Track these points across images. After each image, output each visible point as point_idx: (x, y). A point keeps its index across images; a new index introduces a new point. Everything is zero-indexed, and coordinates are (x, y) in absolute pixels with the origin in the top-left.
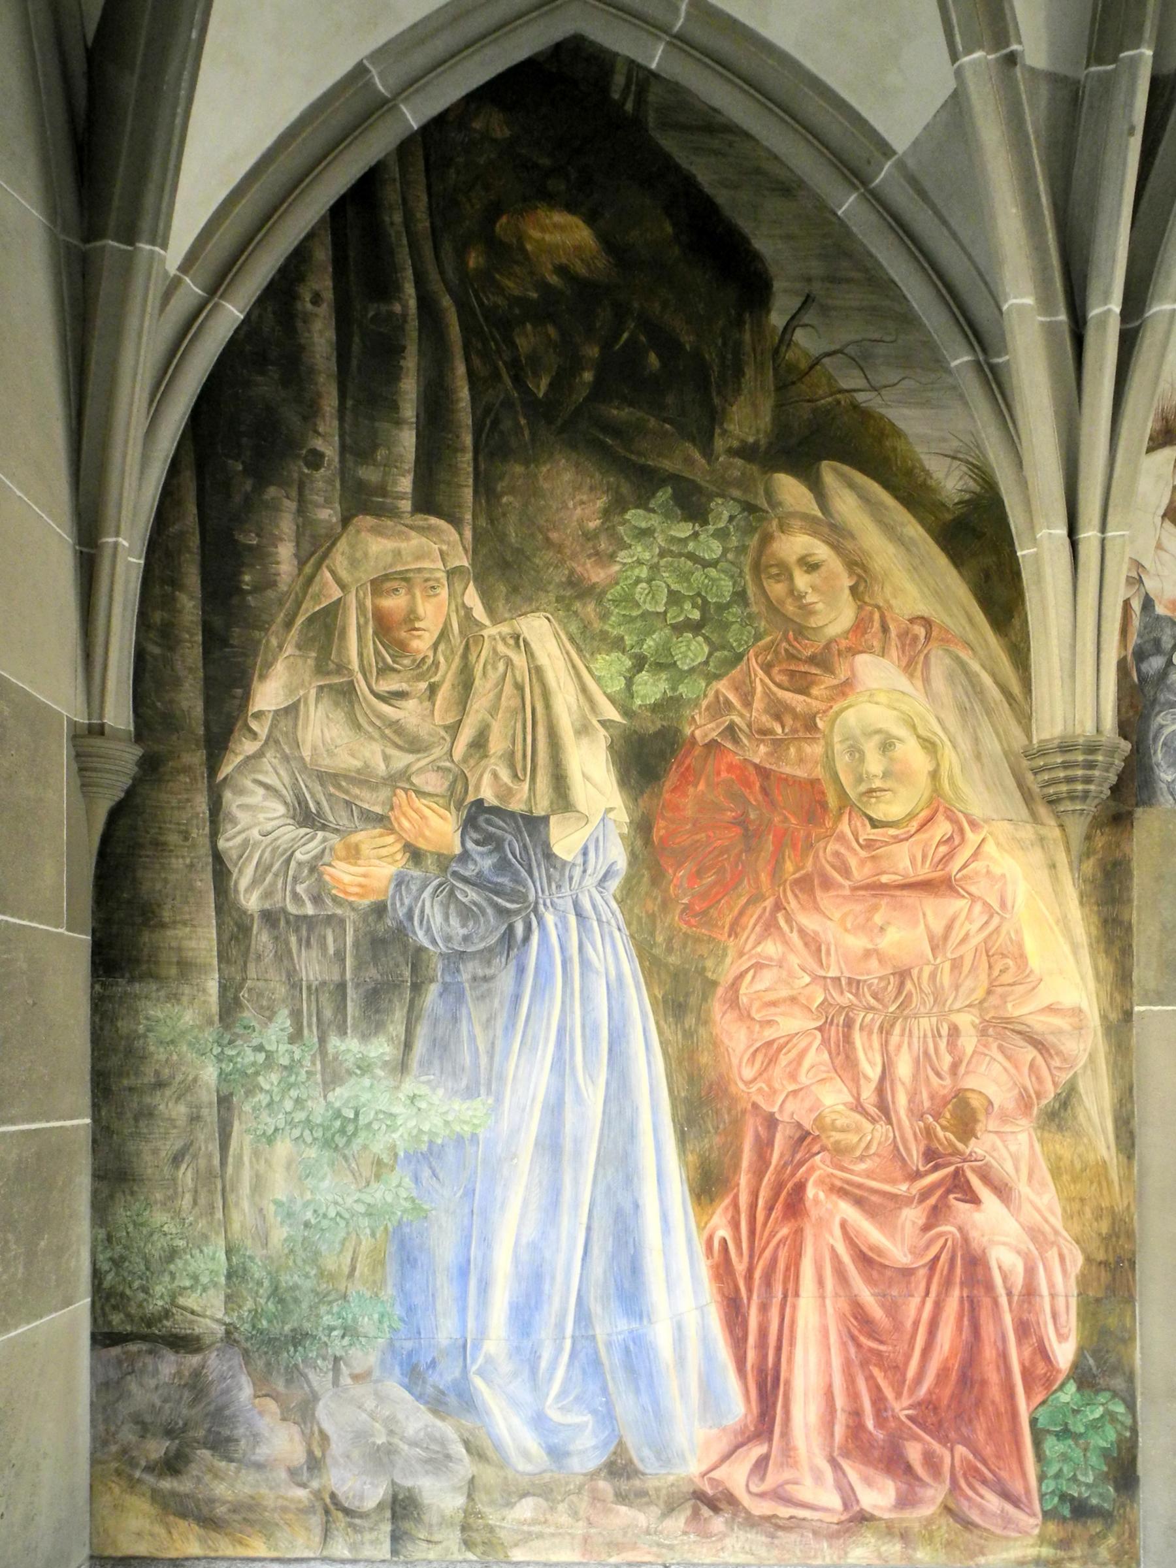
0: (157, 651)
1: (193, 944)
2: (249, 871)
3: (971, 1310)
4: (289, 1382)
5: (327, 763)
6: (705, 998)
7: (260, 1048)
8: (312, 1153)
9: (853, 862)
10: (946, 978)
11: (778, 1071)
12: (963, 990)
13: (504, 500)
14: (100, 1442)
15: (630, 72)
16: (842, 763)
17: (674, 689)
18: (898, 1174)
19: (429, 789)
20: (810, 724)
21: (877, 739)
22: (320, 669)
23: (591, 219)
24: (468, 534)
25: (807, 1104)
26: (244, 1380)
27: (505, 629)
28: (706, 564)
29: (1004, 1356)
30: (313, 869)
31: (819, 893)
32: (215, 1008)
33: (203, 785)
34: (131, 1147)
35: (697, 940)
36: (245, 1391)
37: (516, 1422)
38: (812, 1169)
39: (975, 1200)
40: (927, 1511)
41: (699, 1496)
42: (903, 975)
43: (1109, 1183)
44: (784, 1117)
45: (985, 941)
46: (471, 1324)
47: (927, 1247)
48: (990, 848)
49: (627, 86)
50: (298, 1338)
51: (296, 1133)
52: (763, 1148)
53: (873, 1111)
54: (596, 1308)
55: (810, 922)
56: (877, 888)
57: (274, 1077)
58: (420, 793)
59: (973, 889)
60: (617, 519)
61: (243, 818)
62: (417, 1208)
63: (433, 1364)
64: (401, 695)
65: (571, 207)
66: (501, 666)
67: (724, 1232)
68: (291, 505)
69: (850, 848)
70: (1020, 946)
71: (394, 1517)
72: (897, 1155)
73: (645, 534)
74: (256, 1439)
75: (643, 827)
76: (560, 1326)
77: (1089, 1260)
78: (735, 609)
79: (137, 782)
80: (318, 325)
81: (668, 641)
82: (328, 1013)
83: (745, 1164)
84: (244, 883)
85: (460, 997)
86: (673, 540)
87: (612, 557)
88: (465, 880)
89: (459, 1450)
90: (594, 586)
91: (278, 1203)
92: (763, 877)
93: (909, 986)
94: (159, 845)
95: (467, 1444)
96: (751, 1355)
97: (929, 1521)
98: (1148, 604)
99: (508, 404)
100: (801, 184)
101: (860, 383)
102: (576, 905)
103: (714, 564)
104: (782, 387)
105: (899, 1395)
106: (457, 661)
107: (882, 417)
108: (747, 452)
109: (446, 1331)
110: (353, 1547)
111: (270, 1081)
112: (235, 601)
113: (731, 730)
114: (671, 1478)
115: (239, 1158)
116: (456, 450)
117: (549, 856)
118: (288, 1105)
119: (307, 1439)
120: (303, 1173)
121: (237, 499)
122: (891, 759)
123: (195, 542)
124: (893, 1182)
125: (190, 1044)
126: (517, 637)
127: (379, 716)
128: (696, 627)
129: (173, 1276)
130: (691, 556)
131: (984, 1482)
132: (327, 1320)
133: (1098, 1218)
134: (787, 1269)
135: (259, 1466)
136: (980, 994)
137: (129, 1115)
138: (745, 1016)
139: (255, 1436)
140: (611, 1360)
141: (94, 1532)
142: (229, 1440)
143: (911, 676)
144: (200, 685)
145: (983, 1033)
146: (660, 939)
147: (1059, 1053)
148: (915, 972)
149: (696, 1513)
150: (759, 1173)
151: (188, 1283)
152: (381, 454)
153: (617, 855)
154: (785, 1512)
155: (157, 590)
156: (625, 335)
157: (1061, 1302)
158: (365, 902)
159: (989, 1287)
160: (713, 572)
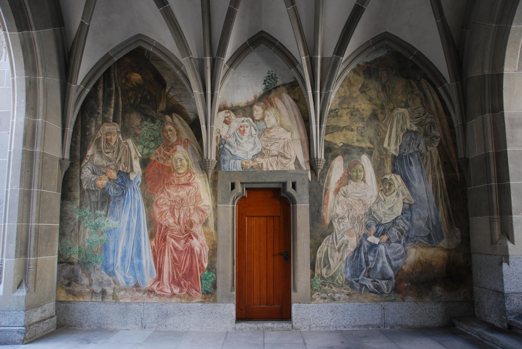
4: (87, 270)
5: (97, 164)
6: (152, 204)
8: (92, 230)
9: (175, 180)
10: (189, 200)
11: (163, 216)
12: (191, 202)
13: (126, 120)
14: (58, 280)
17: (149, 151)
19: (112, 168)
20: (169, 157)
21: (180, 159)
24: (120, 126)
25: (167, 222)
26: (80, 270)
27: (125, 141)
28: (155, 130)
30: (94, 182)
31: (170, 186)
32: (79, 206)
35: (151, 194)
38: (168, 233)
39: (192, 239)
42: (182, 200)
43: (213, 236)
45: (195, 194)
46: (115, 260)
47: (185, 247)
48: (196, 178)
50: (89, 263)
51: (90, 227)
52: (160, 229)
53: (177, 223)
54: (134, 258)
55: (168, 191)
56: (179, 185)
57: (87, 217)
58: (111, 169)
59: (193, 185)
62: (107, 240)
63: (109, 267)
64: (109, 152)
66: (124, 148)
67: (154, 244)
69: (175, 178)
70: (200, 195)
71: (102, 294)
72: (181, 231)
73: (146, 125)
74: (82, 280)
75: (144, 174)
76: (129, 261)
78: (159, 138)
82: (95, 207)
83: (157, 232)
84: (84, 184)
85: (115, 203)
87: (141, 129)
88: (117, 184)
89: (112, 282)
90: (138, 134)
91: (86, 239)
92: (162, 183)
93: (183, 201)
95: (114, 281)
96: (158, 266)
98: (221, 136)
101: (179, 100)
102: (133, 187)
104: (167, 101)
106: (117, 147)
107: (182, 106)
108: (162, 112)
109: (111, 262)
110: (96, 299)
113: (158, 158)
114: (145, 287)
115: (81, 231)
116: (119, 112)
117: (130, 179)
120: (91, 234)
122: (182, 163)
124: (180, 236)
125: (75, 212)
126: (126, 143)
127: (106, 156)
128: (153, 141)
129: (70, 252)
132: (93, 259)
133: (211, 242)
134: (163, 251)
135: (82, 285)
136: (194, 203)
138: (158, 207)
139: (82, 280)
141: (56, 297)
142: (77, 280)
143: (185, 149)
145: (194, 210)
146: (146, 194)
147: (206, 213)
148: (184, 199)
150: (159, 234)
151: (72, 253)
153: (140, 179)
156: (145, 93)
158: (102, 187)
160: (156, 132)
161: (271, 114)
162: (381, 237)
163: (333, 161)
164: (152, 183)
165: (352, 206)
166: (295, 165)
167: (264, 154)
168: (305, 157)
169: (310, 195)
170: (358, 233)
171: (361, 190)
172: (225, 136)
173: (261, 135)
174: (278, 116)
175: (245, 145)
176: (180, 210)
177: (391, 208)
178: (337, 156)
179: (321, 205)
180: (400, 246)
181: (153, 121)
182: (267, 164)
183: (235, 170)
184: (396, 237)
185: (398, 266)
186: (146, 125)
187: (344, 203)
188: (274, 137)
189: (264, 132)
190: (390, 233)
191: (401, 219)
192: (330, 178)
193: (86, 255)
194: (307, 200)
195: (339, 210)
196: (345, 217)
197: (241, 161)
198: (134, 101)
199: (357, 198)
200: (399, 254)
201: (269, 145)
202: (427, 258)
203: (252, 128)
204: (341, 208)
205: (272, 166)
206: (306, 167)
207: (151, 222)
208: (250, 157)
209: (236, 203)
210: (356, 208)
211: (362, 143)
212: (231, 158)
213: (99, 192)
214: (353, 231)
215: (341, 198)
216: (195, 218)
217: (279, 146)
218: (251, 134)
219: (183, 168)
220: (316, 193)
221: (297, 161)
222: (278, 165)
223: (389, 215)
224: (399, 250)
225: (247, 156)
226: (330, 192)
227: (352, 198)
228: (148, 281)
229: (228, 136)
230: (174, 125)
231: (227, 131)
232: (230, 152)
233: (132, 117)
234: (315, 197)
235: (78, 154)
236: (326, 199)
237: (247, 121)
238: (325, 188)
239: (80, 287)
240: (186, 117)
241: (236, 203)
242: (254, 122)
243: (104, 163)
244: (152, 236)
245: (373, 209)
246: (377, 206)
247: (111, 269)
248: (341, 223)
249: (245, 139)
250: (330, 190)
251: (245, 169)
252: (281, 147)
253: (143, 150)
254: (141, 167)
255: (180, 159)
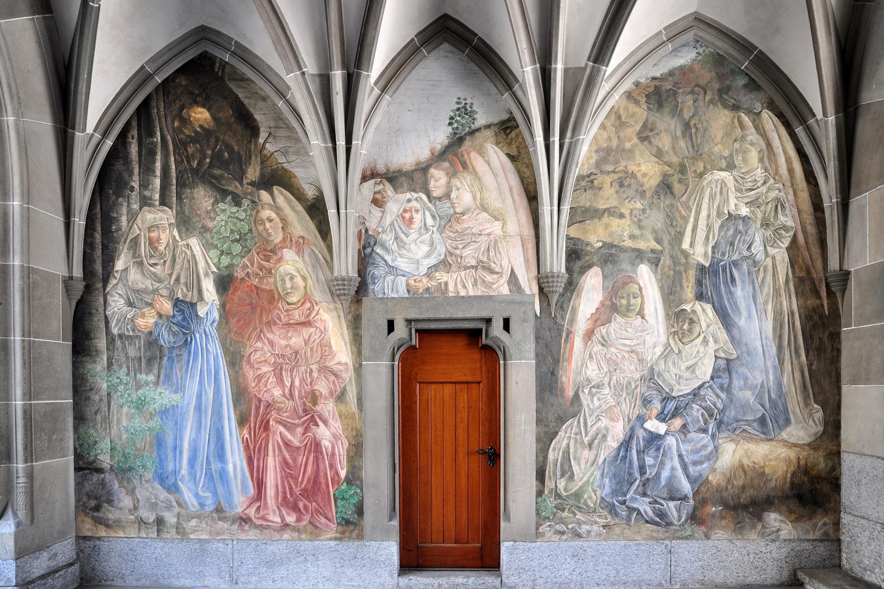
0: (89, 251)
1: (100, 345)
2: (115, 321)
3: (316, 459)
4: (128, 483)
5: (136, 287)
6: (241, 361)
7: (118, 378)
9: (282, 316)
10: (309, 354)
12: (314, 357)
14: (78, 500)
15: (220, 64)
16: (279, 284)
18: (296, 417)
19: (164, 294)
20: (270, 273)
21: (289, 276)
22: (134, 257)
23: (209, 110)
24: (175, 212)
25: (270, 395)
26: (116, 482)
27: (184, 242)
29: (326, 474)
30: (132, 321)
32: (106, 365)
33: (102, 294)
34: (84, 409)
36: (116, 486)
37: (190, 495)
38: (271, 416)
39: (317, 425)
40: (305, 523)
41: (241, 518)
42: (297, 353)
44: (263, 399)
46: (177, 465)
48: (321, 311)
49: (220, 67)
50: (130, 469)
51: (129, 404)
52: (258, 408)
53: (288, 396)
54: (212, 460)
55: (270, 336)
57: (122, 387)
58: (162, 296)
59: (316, 325)
60: (216, 206)
61: (113, 304)
63: (167, 477)
64: (156, 264)
65: (203, 106)
67: (247, 436)
68: (125, 204)
69: (281, 312)
70: (330, 343)
74: (120, 501)
75: (223, 306)
77: (350, 444)
78: (249, 235)
79: (84, 293)
80: (133, 146)
81: (230, 245)
82: (137, 366)
84: (113, 325)
85: (173, 362)
86: (232, 213)
87: (215, 218)
88: (174, 324)
91: (123, 426)
93: (298, 356)
94: (90, 314)
95: (177, 502)
96: (255, 474)
97: (305, 526)
98: (367, 231)
99: (186, 169)
100: (268, 97)
101: (284, 160)
102: (205, 331)
103: (243, 220)
105: (296, 487)
108: (252, 184)
109: (170, 467)
110: (147, 534)
111: (121, 388)
112: (110, 235)
117: (197, 315)
118: (126, 396)
119: (133, 500)
120: (131, 417)
121: (111, 202)
122: (293, 283)
123: (99, 216)
124: (294, 419)
126: (188, 245)
127: (150, 271)
128: (238, 241)
130: (237, 218)
131: (321, 514)
133: (352, 430)
135: (121, 509)
136: (318, 359)
137: (83, 399)
138: (252, 367)
140: (216, 476)
143: (299, 256)
144: (101, 262)
145: (319, 371)
147: (341, 377)
149: (240, 524)
150: (256, 417)
152: (150, 187)
153: (216, 315)
154: (265, 523)
155: (89, 232)
157: (342, 457)
159: (322, 453)
161: (464, 185)
162: (670, 422)
163: (583, 278)
164: (238, 321)
165: (617, 364)
166: (509, 285)
167: (450, 264)
168: (528, 270)
169: (537, 342)
170: (627, 413)
171: (636, 332)
172: (374, 231)
173: (445, 227)
174: (476, 189)
175: (413, 246)
176: (293, 372)
177: (691, 367)
178: (590, 266)
179: (559, 361)
180: (706, 439)
181: (237, 202)
182: (456, 284)
183: (394, 296)
184: (699, 421)
185: (701, 475)
186: (224, 210)
187: (602, 358)
188: (469, 231)
189: (450, 220)
190: (687, 414)
191: (711, 387)
192: (575, 309)
193: (124, 455)
194: (532, 353)
195: (592, 371)
196: (603, 385)
197: (405, 278)
198: (198, 164)
199: (627, 349)
200: (703, 453)
201: (460, 247)
202: (756, 461)
203: (427, 213)
204: (596, 367)
205: (465, 287)
206: (529, 287)
207: (240, 394)
208: (423, 270)
209: (397, 357)
210: (624, 368)
211: (639, 241)
212: (386, 272)
213: (142, 340)
214: (617, 410)
215: (597, 348)
216: (322, 387)
217: (479, 248)
218: (425, 225)
219: (296, 293)
220: (549, 340)
221: (513, 279)
222: (477, 285)
223: (686, 380)
224: (703, 446)
225: (418, 269)
226: (576, 337)
227: (617, 349)
228: (240, 501)
229: (380, 230)
230: (277, 209)
231: (379, 219)
232: (385, 261)
233: (196, 196)
234: (547, 346)
235: (98, 267)
236: (568, 350)
237: (416, 199)
238: (567, 329)
239: (118, 512)
240: (299, 195)
241: (397, 357)
242: (430, 201)
243: (148, 284)
244: (242, 421)
245: (656, 369)
246: (665, 362)
247: (171, 481)
248: (595, 395)
249: (414, 235)
250: (576, 334)
251: (414, 294)
252: (482, 250)
253: (219, 259)
254: (218, 291)
255: (289, 276)
